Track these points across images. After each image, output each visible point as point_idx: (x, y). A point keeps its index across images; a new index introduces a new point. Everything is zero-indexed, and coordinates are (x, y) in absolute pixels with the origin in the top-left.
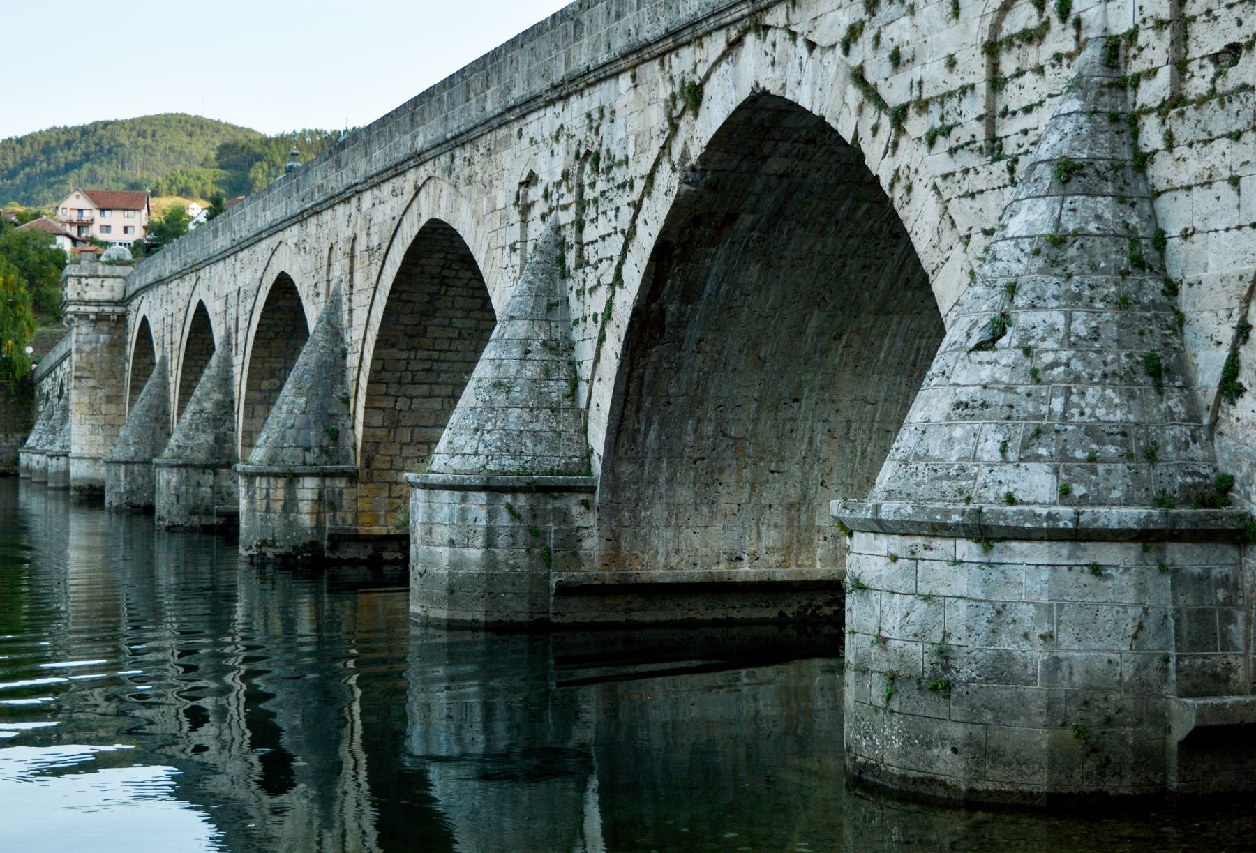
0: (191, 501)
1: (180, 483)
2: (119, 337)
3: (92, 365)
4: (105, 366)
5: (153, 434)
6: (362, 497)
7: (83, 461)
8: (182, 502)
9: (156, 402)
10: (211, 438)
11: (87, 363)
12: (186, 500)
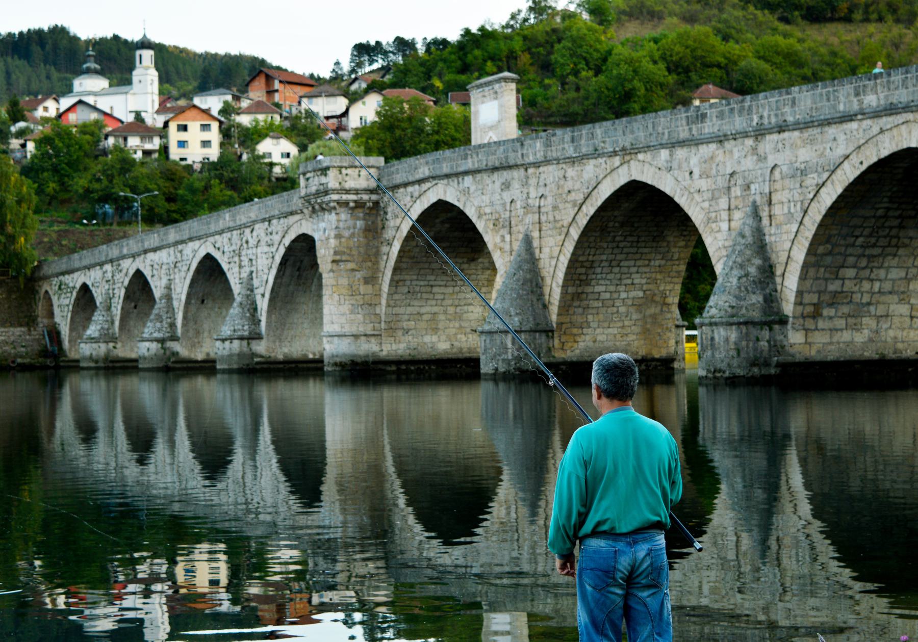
0: (751, 355)
1: (740, 339)
2: (373, 223)
3: (351, 249)
4: (362, 250)
5: (532, 305)
7: (344, 338)
8: (743, 355)
9: (528, 276)
10: (761, 299)
11: (347, 247)
12: (748, 353)
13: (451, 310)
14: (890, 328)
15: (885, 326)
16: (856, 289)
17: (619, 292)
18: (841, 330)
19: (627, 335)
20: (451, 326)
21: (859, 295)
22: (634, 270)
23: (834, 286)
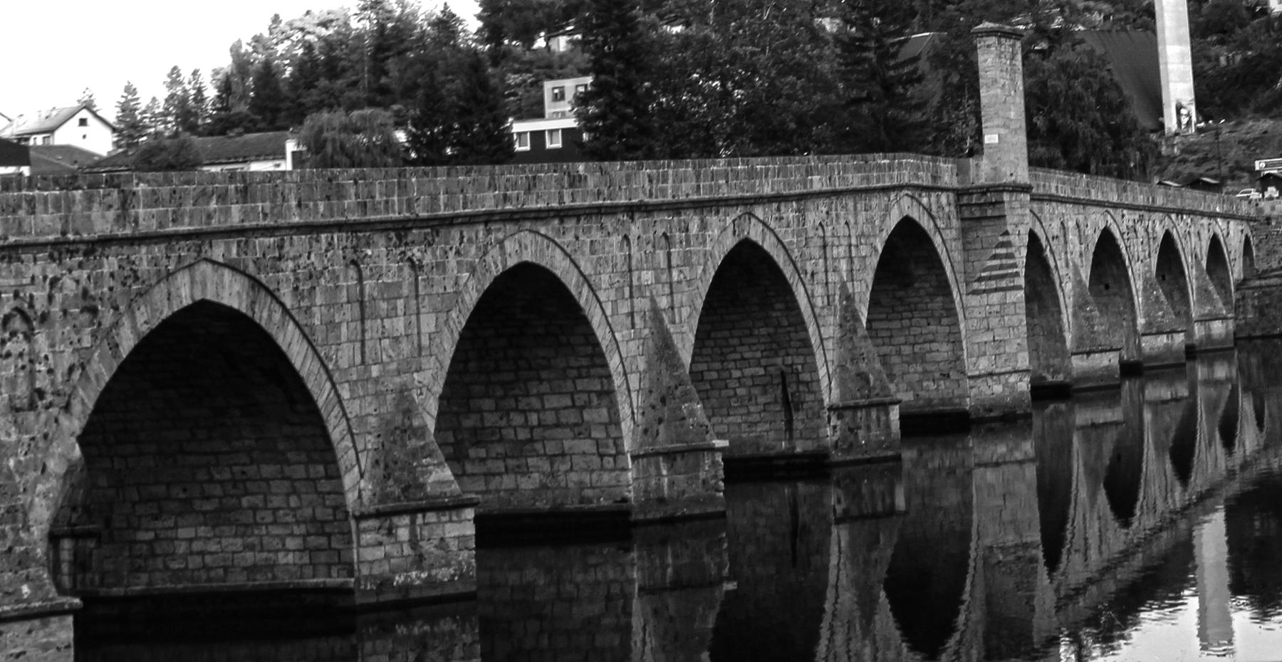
6: (106, 558)
13: (907, 350)
14: (571, 469)
15: (563, 468)
16: (503, 423)
17: (728, 369)
18: (500, 474)
19: (756, 424)
20: (912, 370)
21: (512, 432)
22: (735, 341)
23: (468, 422)
